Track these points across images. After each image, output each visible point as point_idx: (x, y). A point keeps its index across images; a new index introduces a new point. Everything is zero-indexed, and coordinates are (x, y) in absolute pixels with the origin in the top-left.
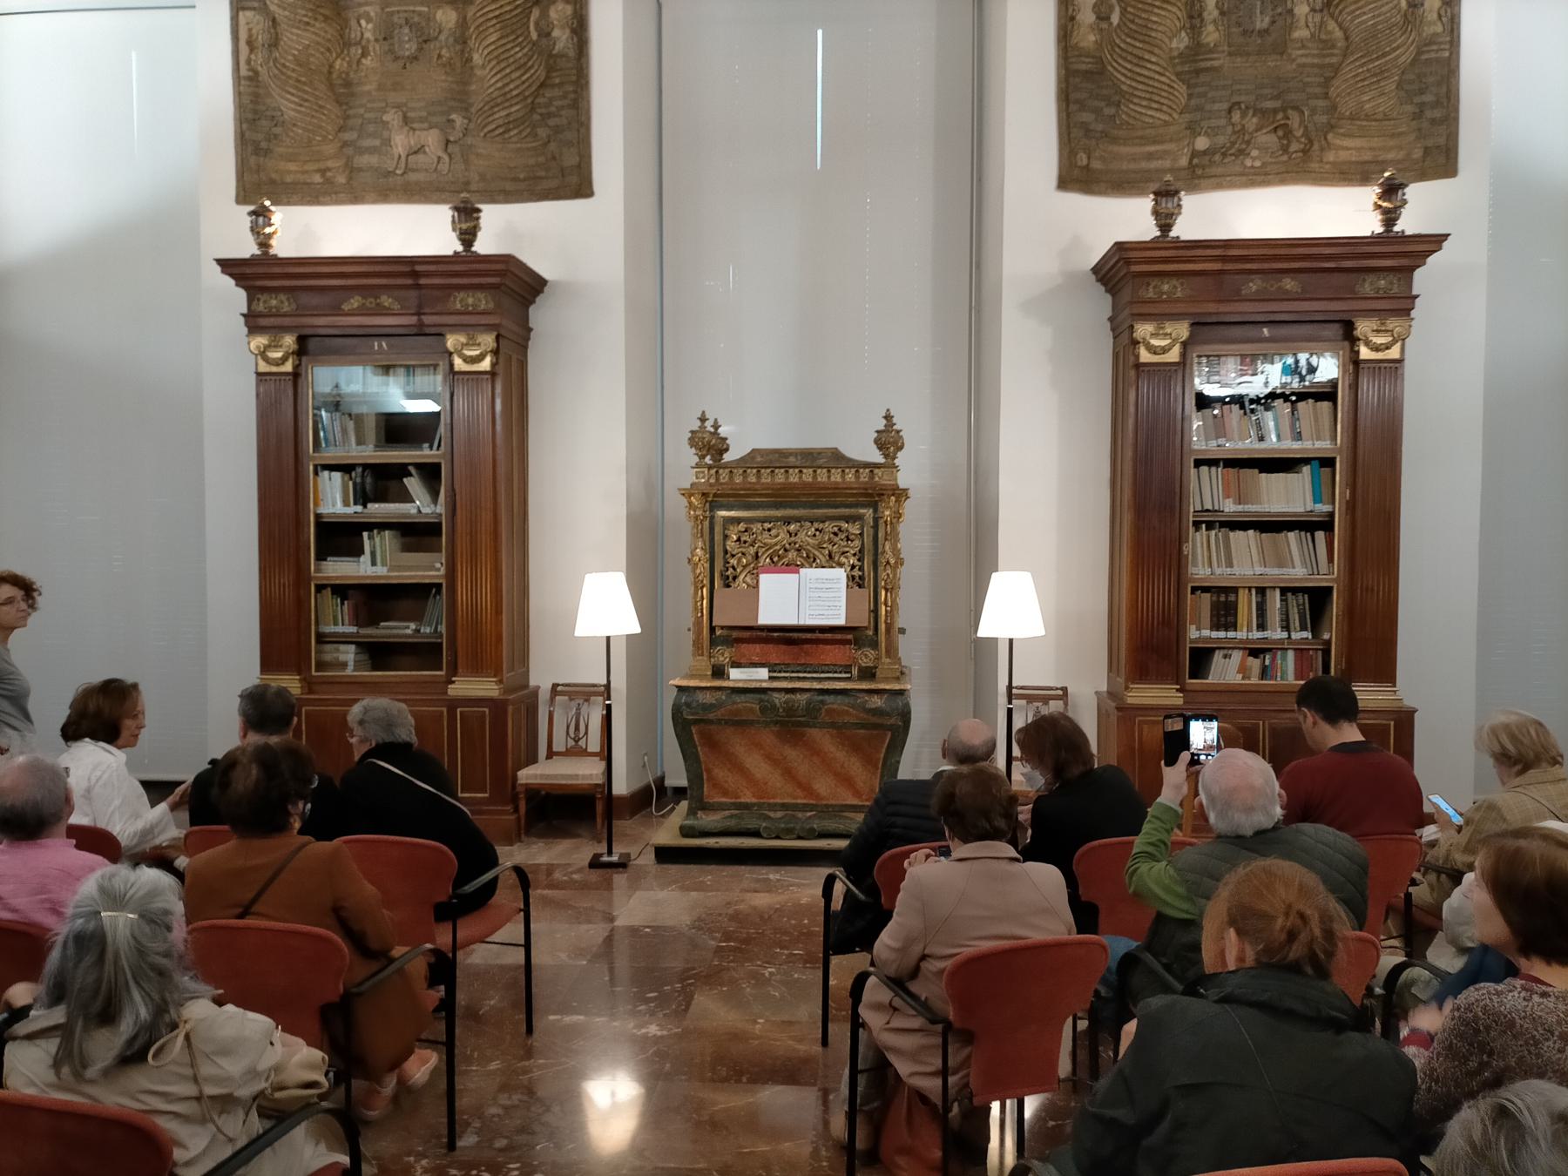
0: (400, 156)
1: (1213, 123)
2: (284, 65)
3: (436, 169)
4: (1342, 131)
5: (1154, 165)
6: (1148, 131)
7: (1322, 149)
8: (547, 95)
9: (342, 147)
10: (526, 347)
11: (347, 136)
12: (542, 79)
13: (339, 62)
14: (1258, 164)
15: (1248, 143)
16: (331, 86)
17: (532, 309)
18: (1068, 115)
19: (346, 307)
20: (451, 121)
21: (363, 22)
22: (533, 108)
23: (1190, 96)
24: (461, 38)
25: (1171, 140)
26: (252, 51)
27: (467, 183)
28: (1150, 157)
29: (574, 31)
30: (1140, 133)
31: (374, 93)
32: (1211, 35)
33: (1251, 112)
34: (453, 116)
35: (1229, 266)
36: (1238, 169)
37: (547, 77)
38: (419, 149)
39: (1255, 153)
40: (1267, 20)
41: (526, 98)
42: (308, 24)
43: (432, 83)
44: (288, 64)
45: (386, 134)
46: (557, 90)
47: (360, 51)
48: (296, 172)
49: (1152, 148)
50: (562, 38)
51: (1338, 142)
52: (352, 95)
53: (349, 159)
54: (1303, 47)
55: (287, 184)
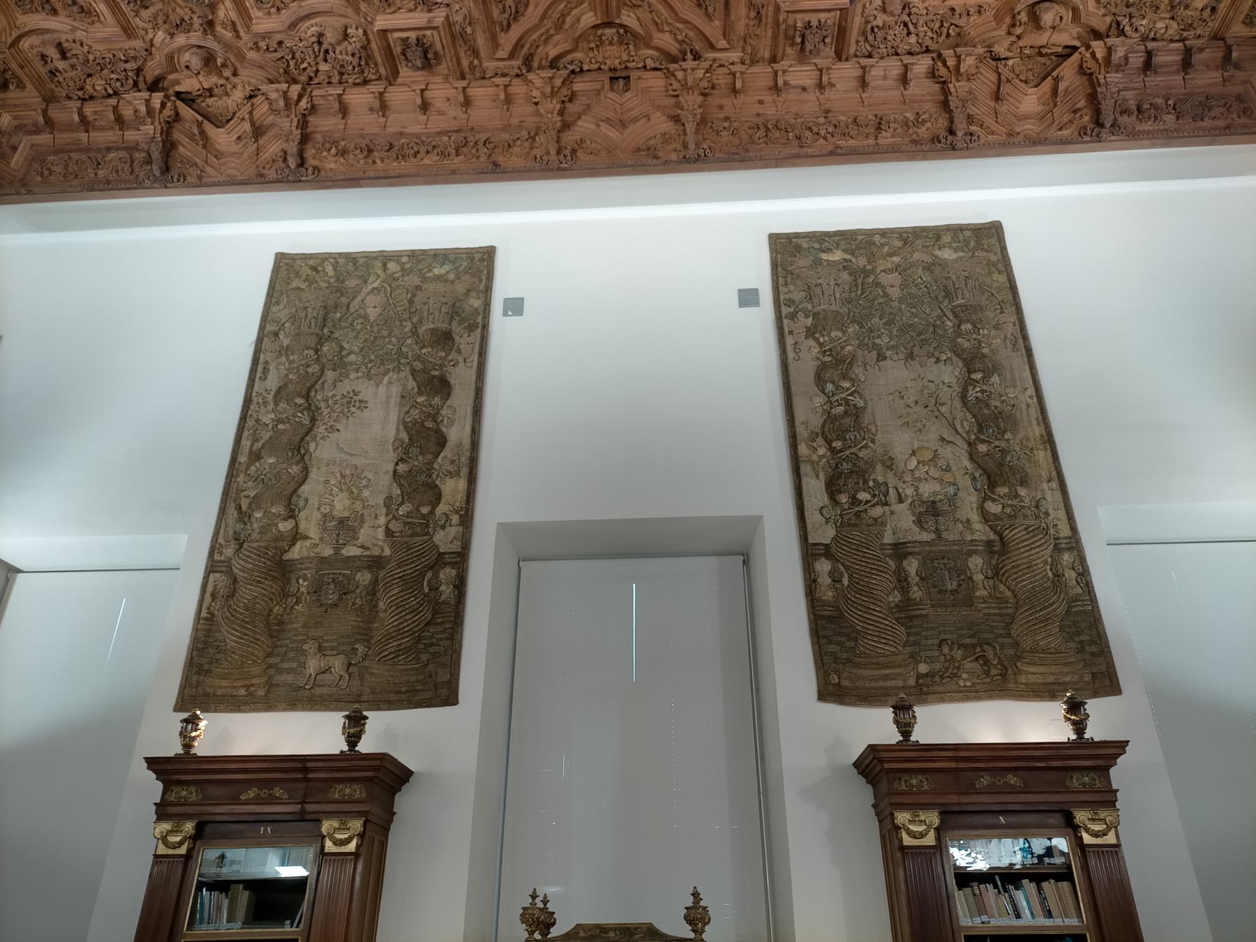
1: (929, 653)
2: (235, 610)
4: (1026, 661)
5: (889, 684)
6: (881, 659)
7: (1015, 674)
9: (267, 668)
10: (387, 830)
11: (272, 660)
14: (969, 684)
15: (958, 668)
17: (397, 795)
18: (820, 646)
19: (243, 797)
21: (301, 581)
22: (419, 639)
23: (909, 635)
24: (372, 590)
25: (899, 666)
26: (213, 600)
27: (361, 695)
28: (886, 678)
29: (456, 587)
30: (875, 660)
31: (299, 630)
32: (916, 593)
33: (956, 646)
35: (961, 765)
36: (954, 687)
39: (965, 676)
40: (955, 583)
41: (414, 633)
42: (259, 582)
43: (346, 621)
45: (302, 659)
47: (294, 600)
48: (227, 687)
49: (886, 672)
50: (446, 591)
51: (1026, 669)
52: (283, 630)
53: (271, 678)
54: (985, 602)
55: (218, 696)
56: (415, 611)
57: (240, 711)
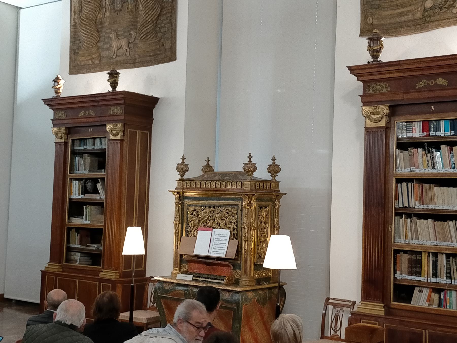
0: (115, 50)
2: (82, 20)
3: (126, 54)
8: (161, 19)
9: (98, 49)
11: (100, 44)
12: (159, 13)
13: (99, 15)
16: (96, 26)
20: (131, 34)
26: (75, 15)
27: (135, 59)
31: (108, 26)
34: (132, 32)
37: (161, 12)
38: (121, 47)
41: (153, 22)
43: (126, 18)
44: (83, 18)
46: (164, 16)
52: (102, 28)
53: (100, 54)
55: (82, 65)
56: (152, 9)
57: (79, 73)
